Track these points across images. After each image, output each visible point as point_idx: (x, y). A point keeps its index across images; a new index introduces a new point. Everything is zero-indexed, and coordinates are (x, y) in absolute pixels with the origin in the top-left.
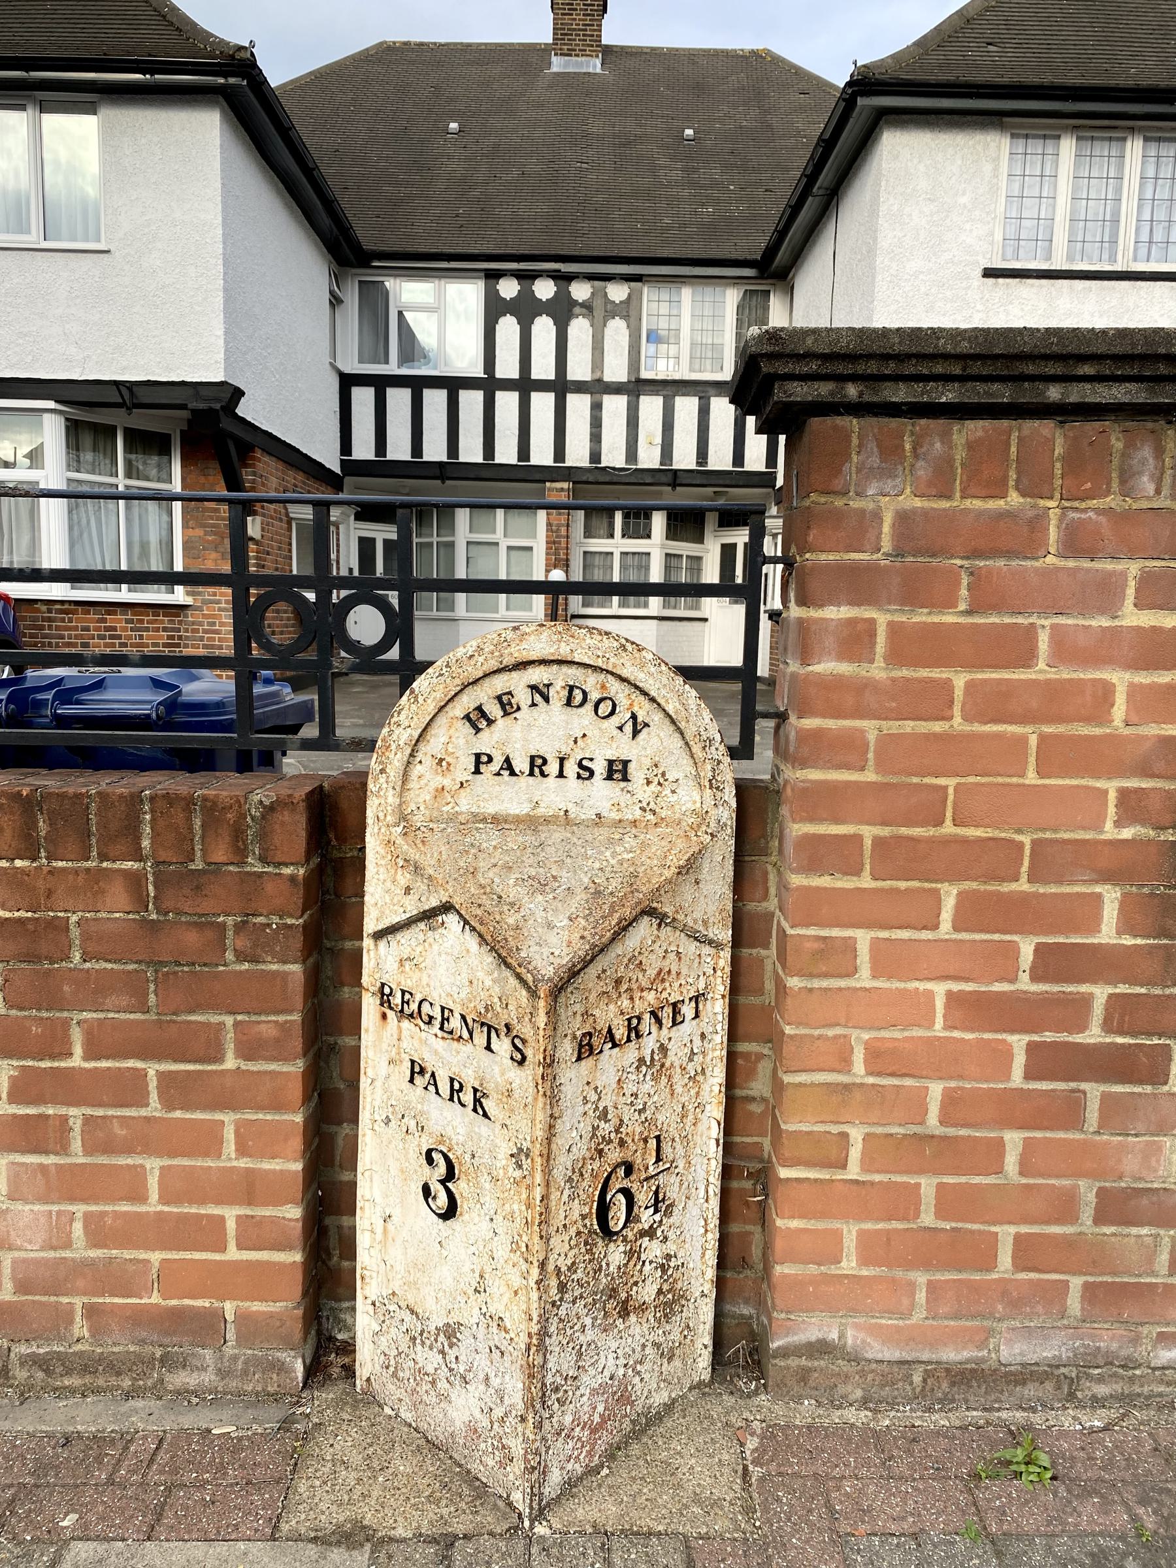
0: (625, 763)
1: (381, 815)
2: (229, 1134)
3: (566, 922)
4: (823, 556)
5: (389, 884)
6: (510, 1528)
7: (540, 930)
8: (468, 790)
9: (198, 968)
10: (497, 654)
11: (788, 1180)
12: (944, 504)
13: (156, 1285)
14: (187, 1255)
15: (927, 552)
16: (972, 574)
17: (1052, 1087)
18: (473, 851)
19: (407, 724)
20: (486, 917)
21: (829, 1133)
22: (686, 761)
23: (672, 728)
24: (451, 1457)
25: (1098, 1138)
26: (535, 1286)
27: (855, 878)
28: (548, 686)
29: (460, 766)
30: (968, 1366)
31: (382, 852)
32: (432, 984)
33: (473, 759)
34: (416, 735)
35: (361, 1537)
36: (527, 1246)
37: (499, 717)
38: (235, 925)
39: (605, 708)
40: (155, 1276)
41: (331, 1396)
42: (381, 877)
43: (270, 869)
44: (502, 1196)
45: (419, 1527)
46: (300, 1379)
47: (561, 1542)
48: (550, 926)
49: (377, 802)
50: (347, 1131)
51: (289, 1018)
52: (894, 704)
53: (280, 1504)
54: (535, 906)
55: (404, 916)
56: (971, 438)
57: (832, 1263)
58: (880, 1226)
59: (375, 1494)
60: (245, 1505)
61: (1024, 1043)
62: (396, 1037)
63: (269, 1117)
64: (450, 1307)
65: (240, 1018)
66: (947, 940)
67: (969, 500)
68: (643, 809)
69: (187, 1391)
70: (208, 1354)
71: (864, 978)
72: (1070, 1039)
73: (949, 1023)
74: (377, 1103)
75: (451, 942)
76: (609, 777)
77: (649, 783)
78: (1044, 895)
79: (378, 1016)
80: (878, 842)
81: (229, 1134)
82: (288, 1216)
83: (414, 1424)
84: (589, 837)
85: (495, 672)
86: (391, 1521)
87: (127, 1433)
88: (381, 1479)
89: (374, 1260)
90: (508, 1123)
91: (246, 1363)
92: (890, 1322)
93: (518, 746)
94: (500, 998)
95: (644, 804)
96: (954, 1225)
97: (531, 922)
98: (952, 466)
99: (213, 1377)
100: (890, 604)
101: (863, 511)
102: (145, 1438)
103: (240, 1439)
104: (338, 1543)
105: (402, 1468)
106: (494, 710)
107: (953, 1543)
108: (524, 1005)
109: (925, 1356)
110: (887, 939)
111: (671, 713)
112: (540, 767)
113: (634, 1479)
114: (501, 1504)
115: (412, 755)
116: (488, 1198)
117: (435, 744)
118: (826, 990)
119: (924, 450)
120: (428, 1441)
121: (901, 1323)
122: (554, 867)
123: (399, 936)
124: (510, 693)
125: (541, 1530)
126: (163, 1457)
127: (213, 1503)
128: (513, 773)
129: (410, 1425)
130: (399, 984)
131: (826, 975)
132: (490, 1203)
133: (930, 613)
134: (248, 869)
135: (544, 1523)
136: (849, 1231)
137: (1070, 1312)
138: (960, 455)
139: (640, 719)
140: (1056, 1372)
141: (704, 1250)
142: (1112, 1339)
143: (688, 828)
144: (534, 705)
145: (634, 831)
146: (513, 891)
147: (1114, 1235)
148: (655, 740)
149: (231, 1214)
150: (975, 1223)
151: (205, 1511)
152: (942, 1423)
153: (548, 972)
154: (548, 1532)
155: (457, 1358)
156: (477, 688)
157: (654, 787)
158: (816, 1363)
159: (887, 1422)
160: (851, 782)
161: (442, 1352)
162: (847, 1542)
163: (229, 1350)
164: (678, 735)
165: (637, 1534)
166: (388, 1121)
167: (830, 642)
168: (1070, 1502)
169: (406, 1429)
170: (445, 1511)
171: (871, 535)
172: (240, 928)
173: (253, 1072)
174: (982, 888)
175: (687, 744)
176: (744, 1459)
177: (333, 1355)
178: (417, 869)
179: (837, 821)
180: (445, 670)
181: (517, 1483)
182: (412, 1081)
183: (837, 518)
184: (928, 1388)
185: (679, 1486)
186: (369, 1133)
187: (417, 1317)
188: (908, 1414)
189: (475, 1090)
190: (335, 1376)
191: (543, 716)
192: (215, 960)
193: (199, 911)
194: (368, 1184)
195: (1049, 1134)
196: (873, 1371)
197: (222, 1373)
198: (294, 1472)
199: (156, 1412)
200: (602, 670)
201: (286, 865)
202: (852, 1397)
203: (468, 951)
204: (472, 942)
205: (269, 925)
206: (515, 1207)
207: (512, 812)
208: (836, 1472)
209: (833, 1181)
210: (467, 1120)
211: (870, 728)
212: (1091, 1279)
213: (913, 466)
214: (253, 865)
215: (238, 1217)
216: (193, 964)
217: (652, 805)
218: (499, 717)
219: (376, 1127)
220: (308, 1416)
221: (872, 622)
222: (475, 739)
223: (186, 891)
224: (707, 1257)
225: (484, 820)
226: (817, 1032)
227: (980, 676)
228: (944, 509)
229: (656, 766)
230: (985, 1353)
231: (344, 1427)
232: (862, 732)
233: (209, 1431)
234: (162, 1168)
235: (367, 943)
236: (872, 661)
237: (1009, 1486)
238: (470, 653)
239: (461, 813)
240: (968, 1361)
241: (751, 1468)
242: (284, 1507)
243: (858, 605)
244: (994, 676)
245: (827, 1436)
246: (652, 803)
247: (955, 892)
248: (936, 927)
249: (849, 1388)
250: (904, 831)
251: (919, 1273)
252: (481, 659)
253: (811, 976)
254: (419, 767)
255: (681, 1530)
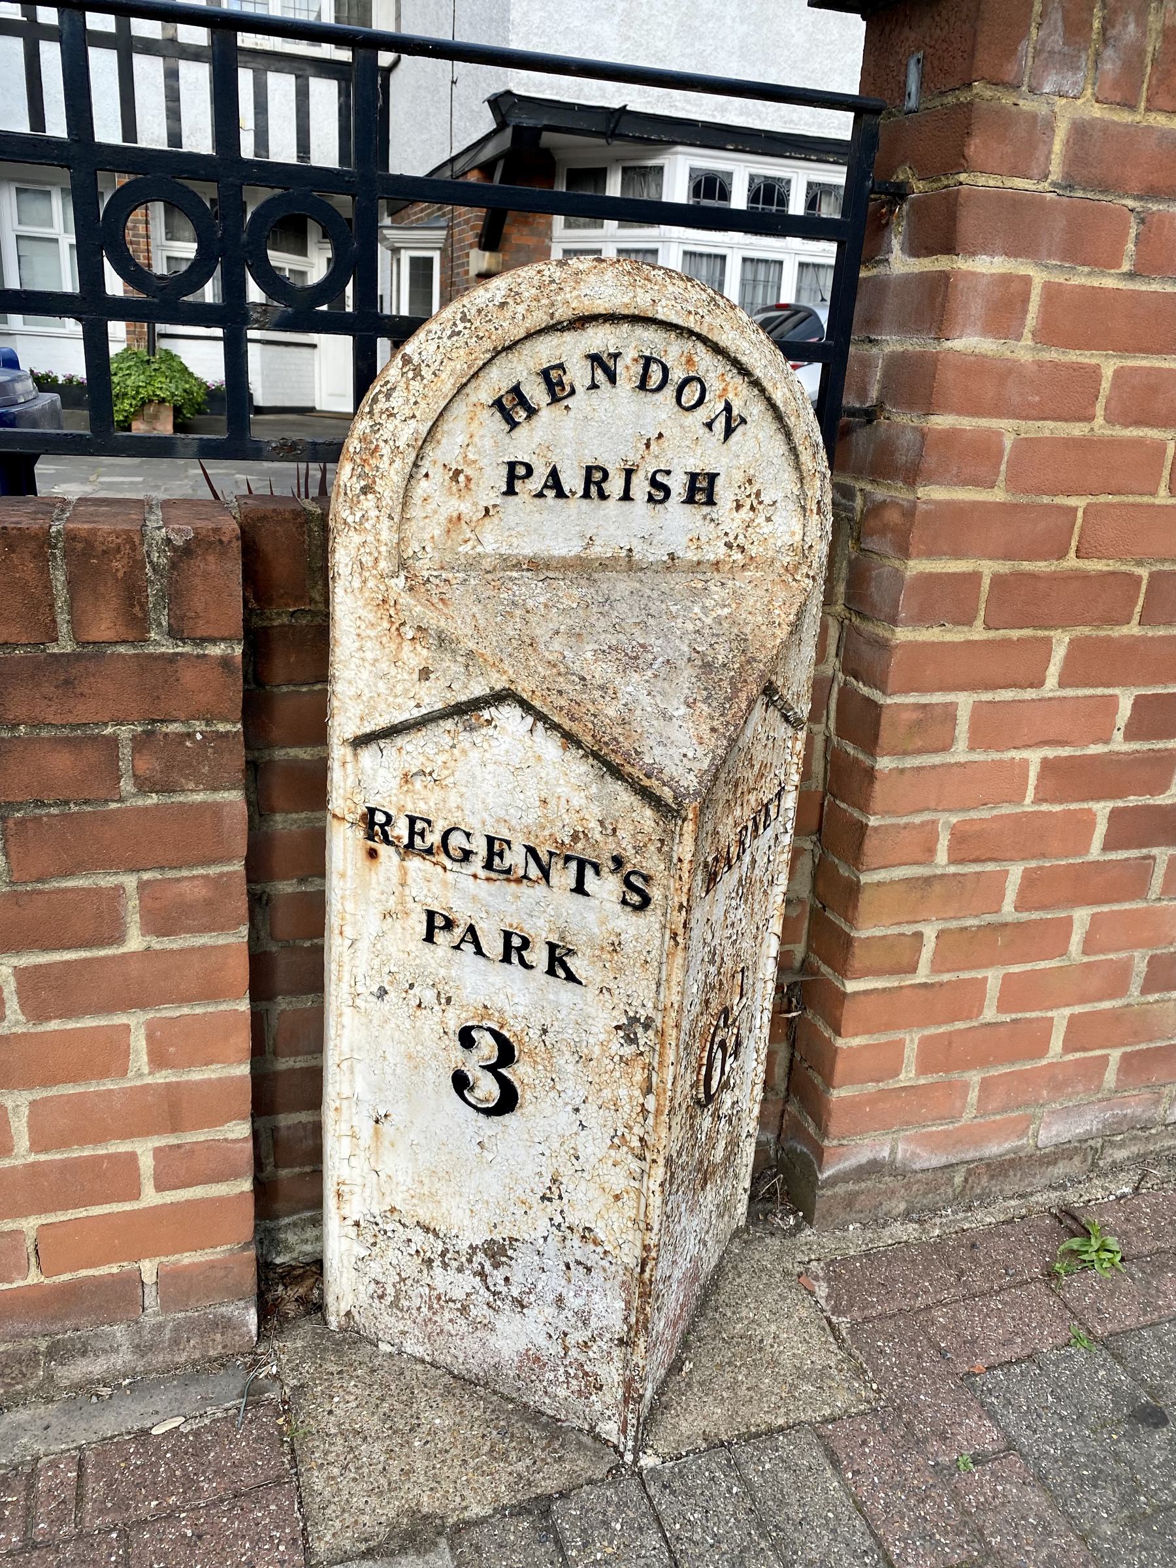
0: (712, 477)
1: (368, 560)
2: (139, 1043)
3: (683, 710)
4: (982, 180)
5: (384, 666)
6: (611, 1468)
7: (655, 722)
8: (496, 520)
9: (74, 809)
10: (545, 301)
11: (856, 994)
12: (1126, 117)
13: (33, 1260)
14: (81, 1213)
15: (1100, 185)
16: (1143, 221)
17: (1126, 856)
18: (518, 612)
19: (408, 413)
20: (578, 711)
21: (903, 935)
22: (788, 477)
23: (775, 426)
24: (495, 1392)
25: (1158, 905)
26: (658, 1189)
27: (966, 629)
28: (616, 356)
29: (485, 483)
30: (1007, 1157)
31: (371, 617)
32: (467, 807)
33: (504, 471)
34: (424, 429)
35: (430, 1534)
36: (641, 1140)
37: (543, 404)
38: (134, 739)
39: (691, 395)
40: (31, 1249)
41: (299, 1344)
42: (369, 655)
43: (187, 649)
44: (597, 1079)
45: (497, 1499)
46: (253, 1328)
47: (680, 1471)
48: (666, 717)
49: (357, 539)
50: (284, 1006)
51: (226, 869)
52: (1037, 399)
53: (298, 1515)
54: (632, 686)
55: (416, 713)
56: (1168, 22)
57: (892, 1078)
58: (943, 1029)
59: (420, 1465)
60: (248, 1528)
61: (1108, 810)
62: (395, 880)
63: (199, 1010)
64: (497, 1220)
65: (146, 876)
66: (1050, 699)
67: (1154, 115)
68: (729, 545)
69: (91, 1382)
70: (119, 1331)
71: (960, 752)
72: (1151, 802)
73: (1040, 796)
74: (360, 972)
75: (504, 747)
76: (690, 500)
77: (739, 507)
78: (1152, 638)
79: (361, 854)
80: (998, 581)
81: (139, 1043)
82: (231, 1136)
83: (428, 1359)
84: (664, 587)
85: (540, 332)
86: (458, 1499)
87: (22, 1463)
88: (417, 1444)
89: (357, 1171)
90: (612, 985)
91: (176, 1329)
92: (941, 1128)
93: (568, 451)
94: (601, 823)
95: (731, 538)
96: (1014, 1016)
97: (638, 712)
98: (1142, 62)
99: (128, 1357)
100: (1049, 256)
101: (1034, 117)
102: (53, 1465)
103: (197, 1433)
104: (403, 1550)
105: (437, 1421)
106: (536, 393)
107: (1071, 1356)
108: (647, 830)
109: (970, 1155)
110: (990, 702)
111: (779, 403)
112: (598, 484)
113: (720, 1366)
114: (587, 1440)
115: (416, 465)
116: (571, 1084)
117: (448, 449)
118: (919, 769)
119: (1114, 32)
120: (455, 1377)
121: (951, 1127)
122: (637, 631)
123: (400, 741)
124: (561, 366)
125: (648, 1461)
126: (95, 1489)
127: (200, 1537)
128: (561, 494)
129: (423, 1361)
130: (401, 808)
131: (920, 752)
132: (574, 1090)
133: (1089, 274)
134: (151, 649)
135: (650, 1451)
136: (912, 1041)
137: (1106, 1085)
138: (1153, 44)
139: (735, 412)
140: (1084, 1146)
141: (754, 1084)
142: (1137, 1105)
143: (782, 571)
144: (594, 386)
145: (717, 576)
146: (600, 671)
147: (1157, 1001)
148: (752, 443)
149: (145, 1151)
150: (1034, 1011)
151: (192, 1553)
152: (988, 1220)
153: (690, 782)
154: (658, 1461)
155: (507, 1279)
156: (513, 356)
157: (745, 514)
158: (863, 1185)
159: (937, 1232)
160: (979, 502)
161: (482, 1274)
162: (973, 1384)
163: (149, 1319)
164: (780, 437)
165: (757, 1435)
166: (382, 992)
167: (977, 308)
168: (1149, 1283)
169: (419, 1367)
170: (520, 1467)
171: (1040, 154)
172: (141, 743)
173: (172, 951)
174: (1094, 633)
175: (793, 450)
176: (822, 1311)
177: (281, 1288)
178: (443, 641)
179: (957, 555)
180: (460, 326)
181: (608, 1413)
182: (429, 938)
183: (1004, 120)
184: (968, 1186)
185: (776, 1363)
186: (348, 1011)
187: (436, 1235)
188: (951, 1218)
189: (552, 947)
190: (291, 1314)
191: (606, 404)
192: (102, 793)
193: (72, 719)
194: (346, 1077)
195: (1116, 907)
196: (919, 1181)
197: (140, 1349)
198: (294, 1462)
199: (54, 1422)
200: (691, 333)
201: (214, 641)
202: (895, 1212)
203: (539, 758)
204: (549, 746)
205: (190, 736)
206: (623, 1092)
207: (556, 553)
208: (920, 1302)
209: (901, 987)
210: (532, 985)
211: (1008, 430)
212: (1129, 1049)
213: (1098, 54)
214: (157, 643)
215: (157, 1151)
216: (67, 803)
217: (741, 540)
218: (543, 404)
219: (358, 1002)
220: (276, 1377)
221: (1027, 280)
222: (507, 440)
223: (48, 689)
224: (755, 1093)
225: (517, 566)
226: (903, 820)
227: (1130, 363)
228: (1126, 125)
229: (750, 482)
230: (1024, 1141)
231: (337, 1383)
232: (999, 434)
233: (145, 1432)
234: (33, 1104)
235: (338, 752)
236: (1019, 337)
237: (1086, 1278)
238: (499, 299)
239: (486, 556)
240: (1008, 1152)
241: (834, 1319)
242: (305, 1518)
243: (1016, 257)
244: (1145, 363)
245: (889, 1263)
246: (741, 536)
247: (1067, 640)
248: (1040, 684)
249: (894, 1203)
250: (1026, 566)
251: (975, 1072)
252: (521, 309)
253: (905, 753)
254: (424, 483)
255: (803, 1418)
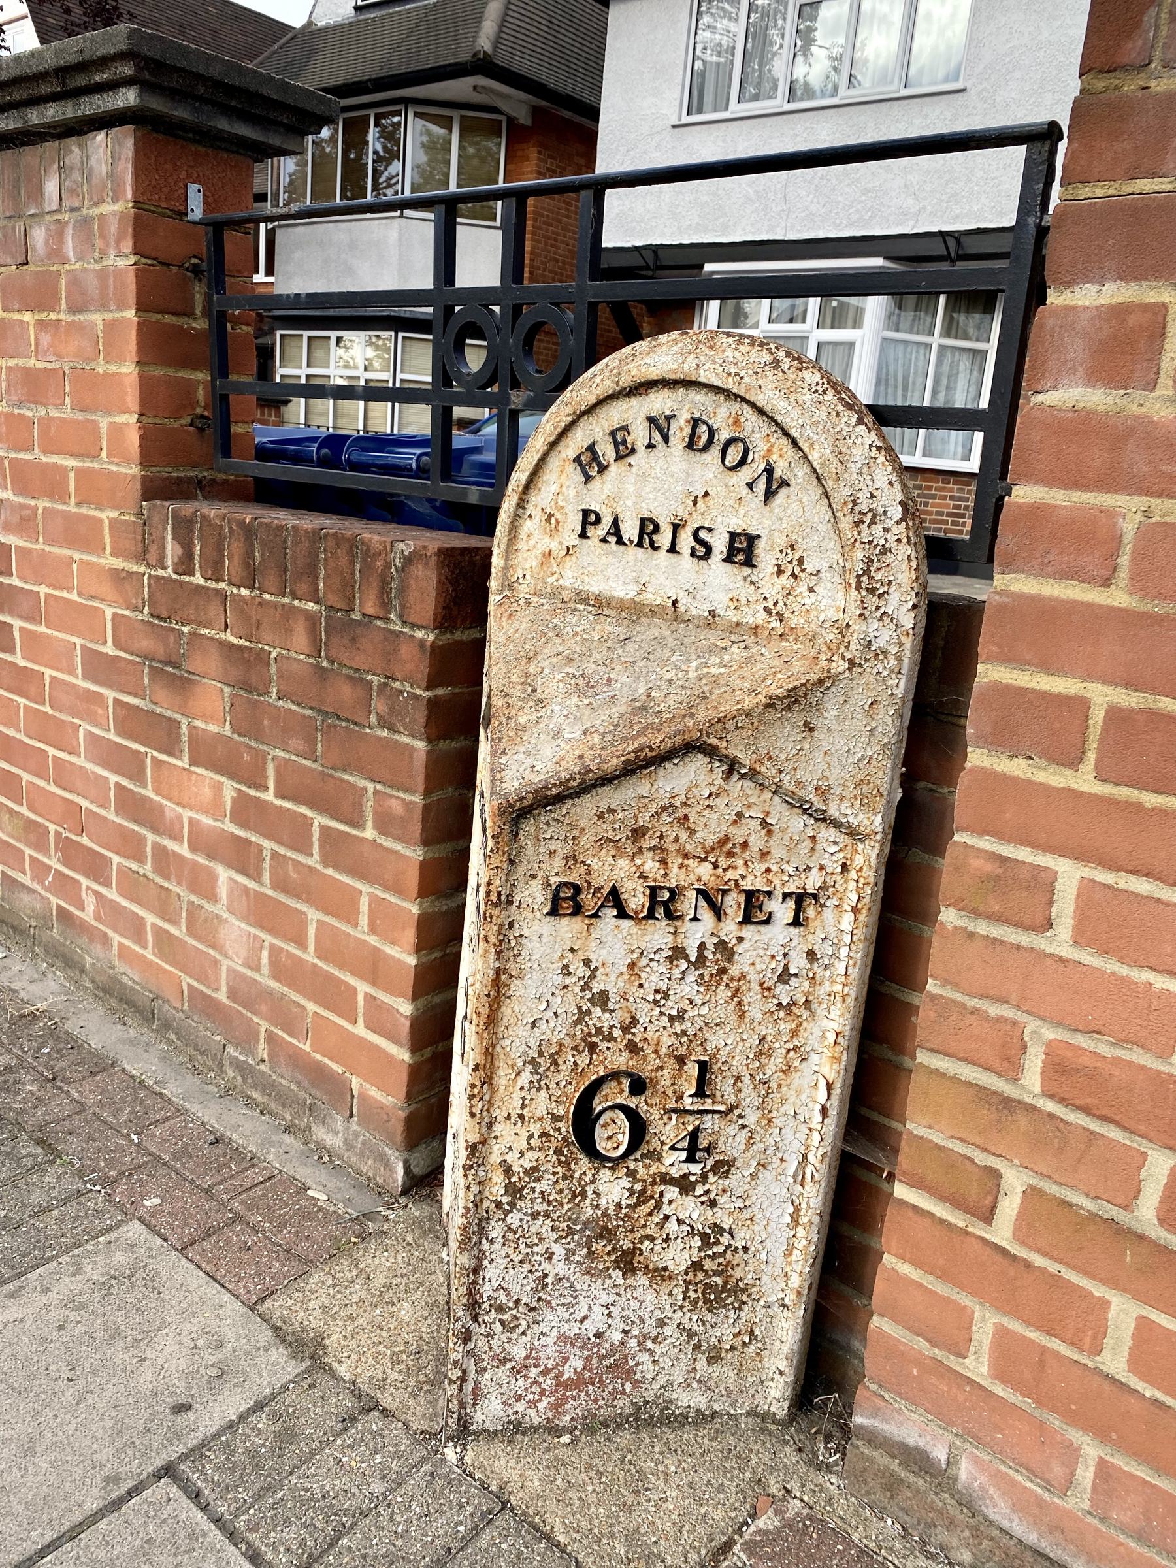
8: (574, 558)
21: (972, 1161)
27: (1069, 772)
28: (669, 419)
33: (580, 516)
39: (734, 455)
48: (557, 734)
58: (1033, 1335)
59: (360, 1321)
76: (729, 559)
77: (780, 572)
80: (1115, 715)
82: (402, 1010)
86: (345, 1354)
93: (629, 503)
106: (607, 451)
110: (1109, 887)
113: (590, 1467)
128: (620, 542)
131: (998, 918)
136: (983, 1319)
139: (777, 474)
148: (794, 507)
167: (1076, 349)
176: (740, 1532)
179: (1048, 667)
191: (661, 462)
205: (402, 692)
209: (967, 1233)
218: (612, 461)
225: (585, 601)
226: (972, 1003)
232: (1111, 514)
236: (1152, 385)
246: (781, 603)
253: (975, 913)
254: (528, 522)
255: (580, 1557)
